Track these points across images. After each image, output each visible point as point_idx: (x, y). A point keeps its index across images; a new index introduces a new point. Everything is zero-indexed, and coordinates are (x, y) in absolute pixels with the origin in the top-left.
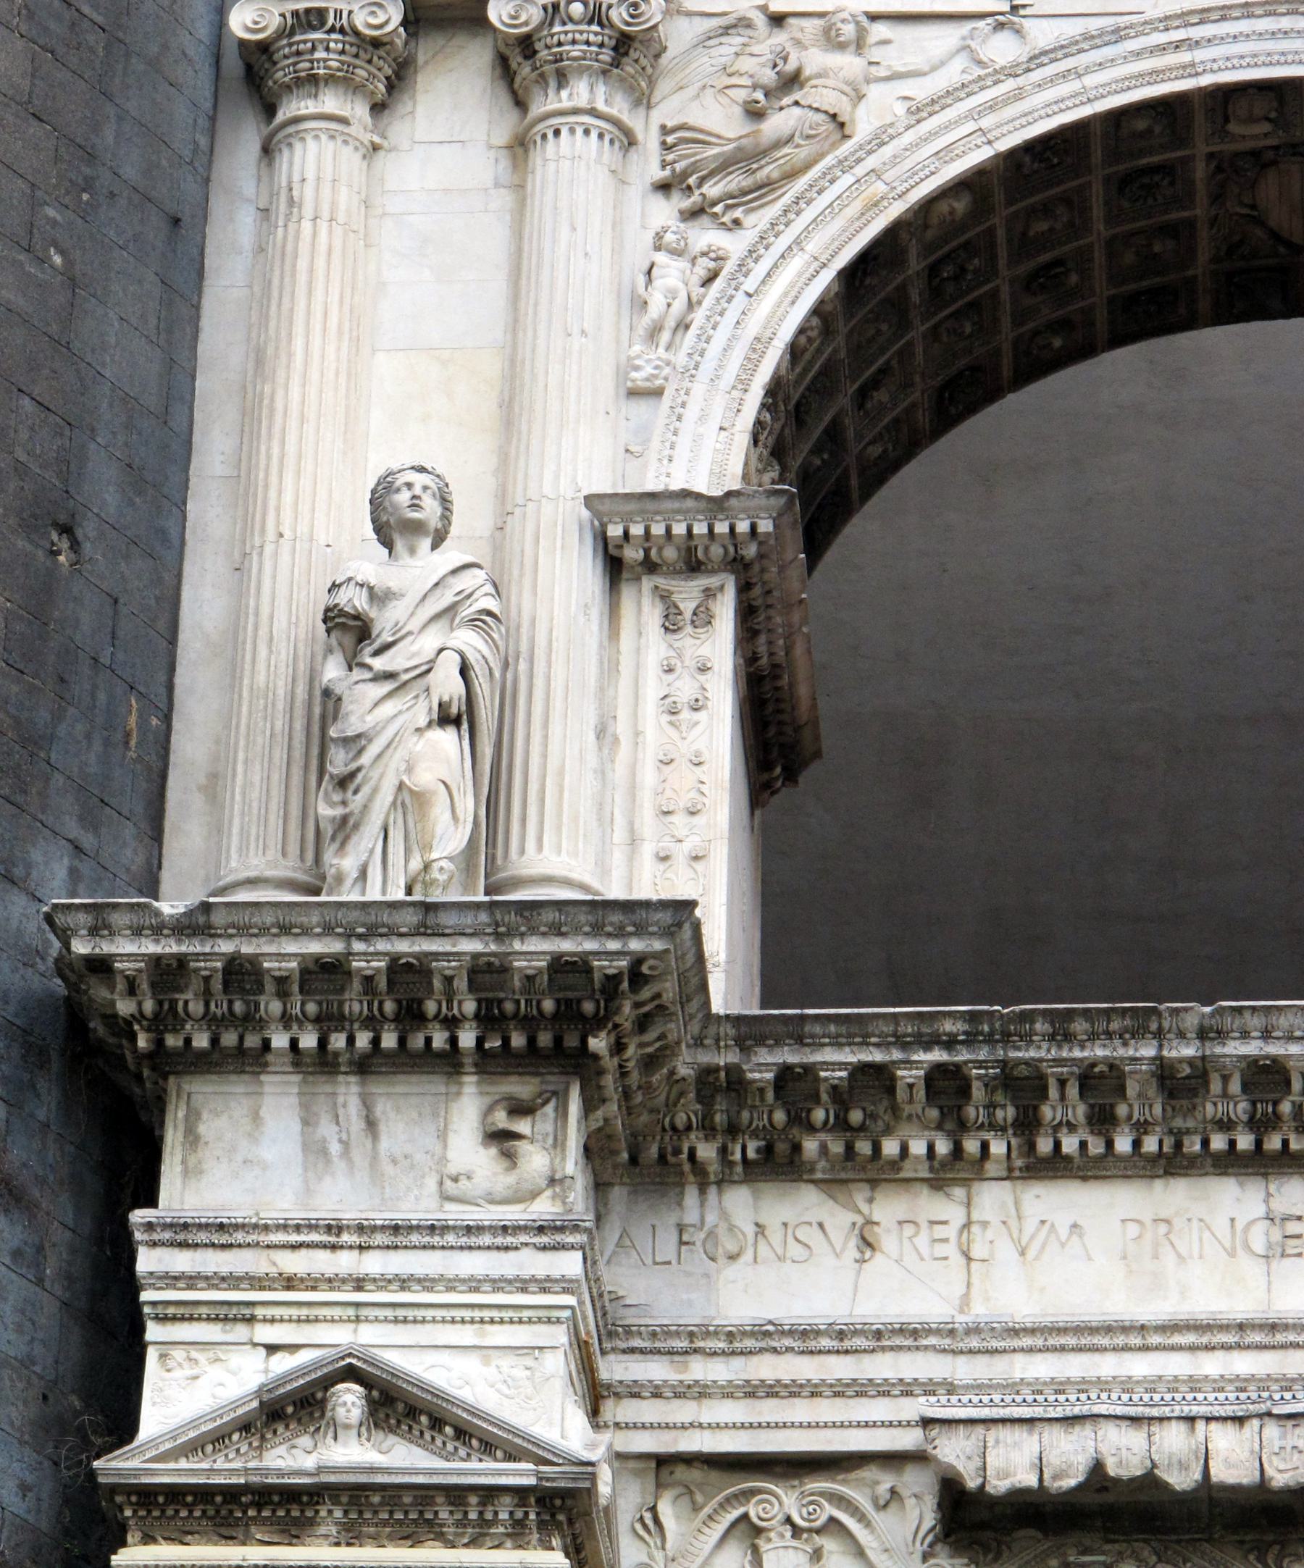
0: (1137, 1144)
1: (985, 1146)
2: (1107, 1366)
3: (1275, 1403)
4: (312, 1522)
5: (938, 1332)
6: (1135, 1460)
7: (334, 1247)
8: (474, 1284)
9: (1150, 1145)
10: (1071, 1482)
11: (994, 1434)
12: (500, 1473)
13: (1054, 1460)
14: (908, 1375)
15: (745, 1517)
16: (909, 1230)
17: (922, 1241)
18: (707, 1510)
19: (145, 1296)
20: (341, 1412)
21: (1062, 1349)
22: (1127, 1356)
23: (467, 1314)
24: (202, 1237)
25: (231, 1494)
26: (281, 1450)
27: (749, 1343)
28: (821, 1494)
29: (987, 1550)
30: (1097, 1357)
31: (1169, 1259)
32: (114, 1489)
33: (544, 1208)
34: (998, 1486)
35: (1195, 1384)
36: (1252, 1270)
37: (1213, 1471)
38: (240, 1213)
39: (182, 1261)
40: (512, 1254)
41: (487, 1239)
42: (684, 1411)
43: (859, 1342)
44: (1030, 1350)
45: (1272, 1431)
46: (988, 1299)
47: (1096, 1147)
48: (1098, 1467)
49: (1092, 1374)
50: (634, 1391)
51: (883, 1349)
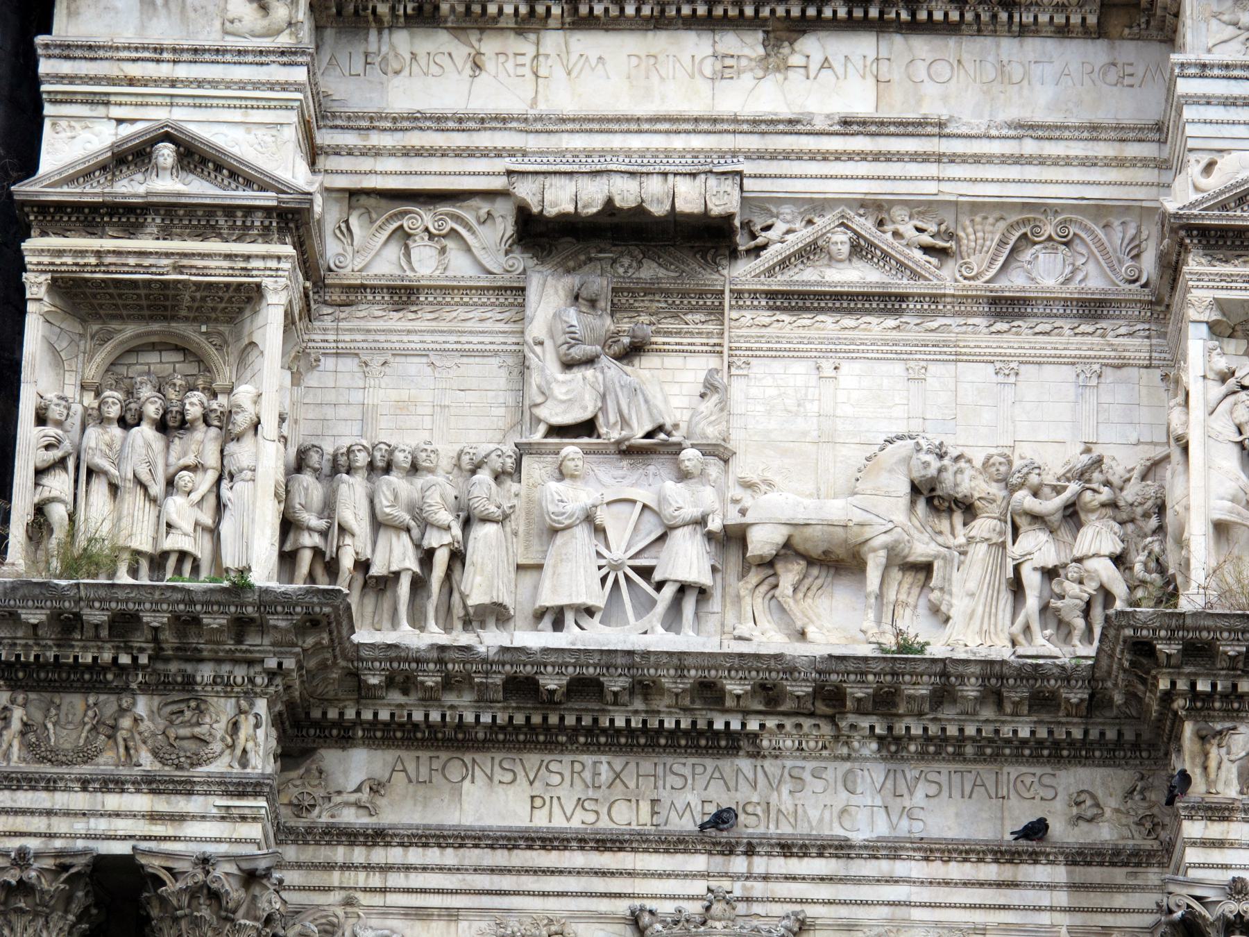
0: (638, 10)
1: (548, 9)
2: (617, 141)
3: (715, 165)
4: (142, 225)
5: (518, 120)
6: (632, 198)
7: (158, 61)
8: (242, 85)
9: (646, 11)
10: (594, 210)
11: (549, 181)
12: (255, 198)
13: (584, 197)
14: (499, 145)
15: (401, 227)
16: (502, 58)
17: (510, 65)
18: (379, 223)
19: (44, 88)
20: (161, 160)
21: (591, 131)
22: (629, 136)
23: (238, 103)
24: (79, 53)
25: (94, 208)
26: (125, 182)
27: (406, 124)
28: (447, 215)
29: (543, 249)
30: (611, 136)
31: (655, 79)
32: (24, 203)
33: (284, 40)
34: (551, 211)
35: (668, 153)
36: (704, 87)
37: (677, 205)
38: (102, 39)
39: (66, 67)
40: (265, 68)
41: (250, 58)
42: (366, 164)
43: (471, 125)
44: (572, 131)
45: (712, 181)
46: (547, 100)
47: (614, 11)
48: (609, 202)
49: (608, 146)
50: (337, 151)
51: (485, 129)
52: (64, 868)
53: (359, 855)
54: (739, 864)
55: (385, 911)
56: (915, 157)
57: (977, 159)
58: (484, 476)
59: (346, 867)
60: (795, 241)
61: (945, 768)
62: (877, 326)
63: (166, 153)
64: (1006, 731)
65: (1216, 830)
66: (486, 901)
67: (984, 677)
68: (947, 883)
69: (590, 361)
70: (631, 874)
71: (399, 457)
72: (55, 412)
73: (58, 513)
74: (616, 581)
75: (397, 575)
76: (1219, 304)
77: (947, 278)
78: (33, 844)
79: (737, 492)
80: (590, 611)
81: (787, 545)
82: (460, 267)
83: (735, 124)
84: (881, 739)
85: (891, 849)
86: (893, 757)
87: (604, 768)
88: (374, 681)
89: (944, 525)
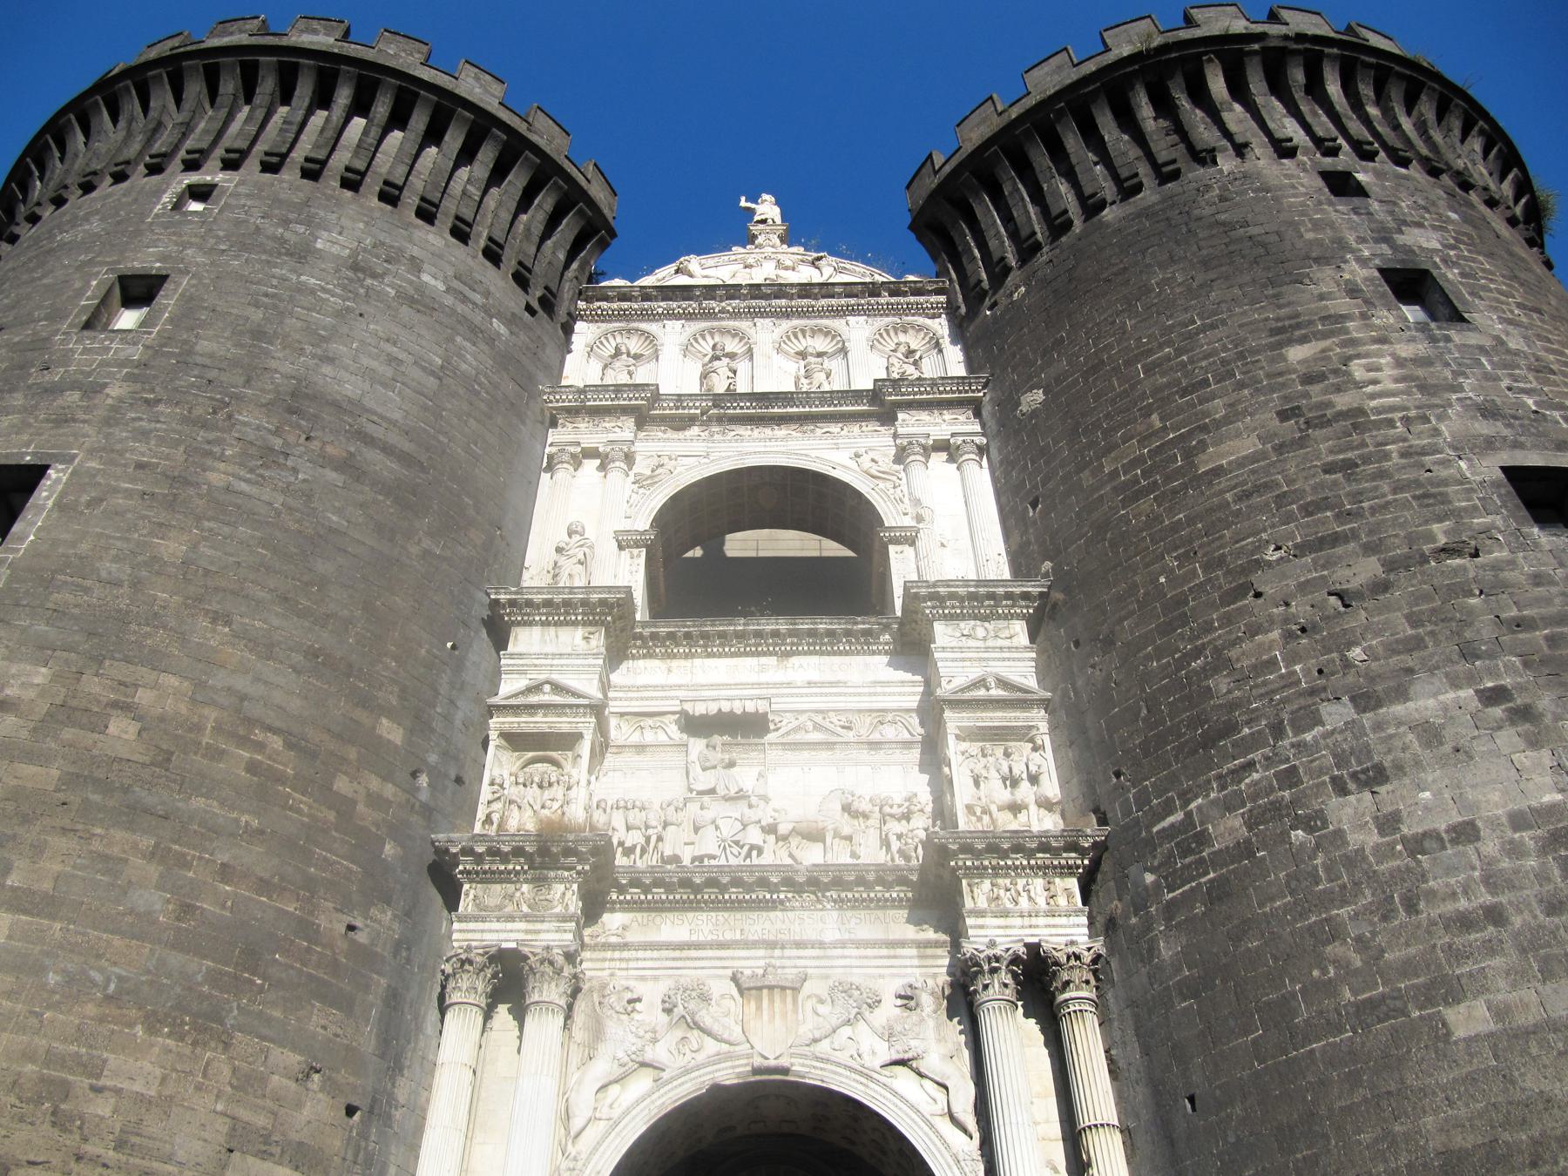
25: (518, 707)
34: (697, 714)
42: (626, 703)
50: (615, 699)
52: (487, 953)
53: (617, 954)
54: (777, 952)
55: (627, 978)
56: (836, 694)
57: (859, 694)
58: (672, 808)
59: (612, 960)
60: (790, 726)
61: (862, 912)
62: (824, 755)
63: (547, 688)
64: (887, 895)
65: (980, 921)
66: (671, 972)
67: (877, 871)
68: (866, 957)
69: (714, 767)
70: (733, 958)
71: (638, 803)
72: (498, 781)
73: (495, 817)
74: (725, 848)
75: (634, 847)
76: (959, 727)
77: (850, 736)
78: (474, 944)
79: (773, 814)
80: (714, 857)
81: (793, 830)
82: (662, 737)
83: (768, 685)
84: (835, 901)
85: (843, 944)
86: (841, 908)
87: (720, 918)
88: (624, 882)
89: (856, 822)
